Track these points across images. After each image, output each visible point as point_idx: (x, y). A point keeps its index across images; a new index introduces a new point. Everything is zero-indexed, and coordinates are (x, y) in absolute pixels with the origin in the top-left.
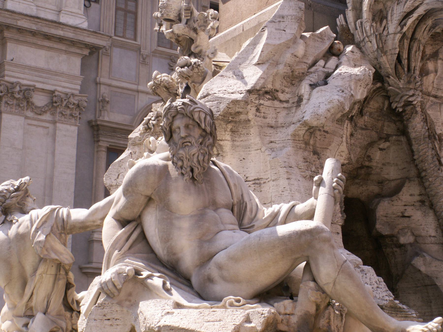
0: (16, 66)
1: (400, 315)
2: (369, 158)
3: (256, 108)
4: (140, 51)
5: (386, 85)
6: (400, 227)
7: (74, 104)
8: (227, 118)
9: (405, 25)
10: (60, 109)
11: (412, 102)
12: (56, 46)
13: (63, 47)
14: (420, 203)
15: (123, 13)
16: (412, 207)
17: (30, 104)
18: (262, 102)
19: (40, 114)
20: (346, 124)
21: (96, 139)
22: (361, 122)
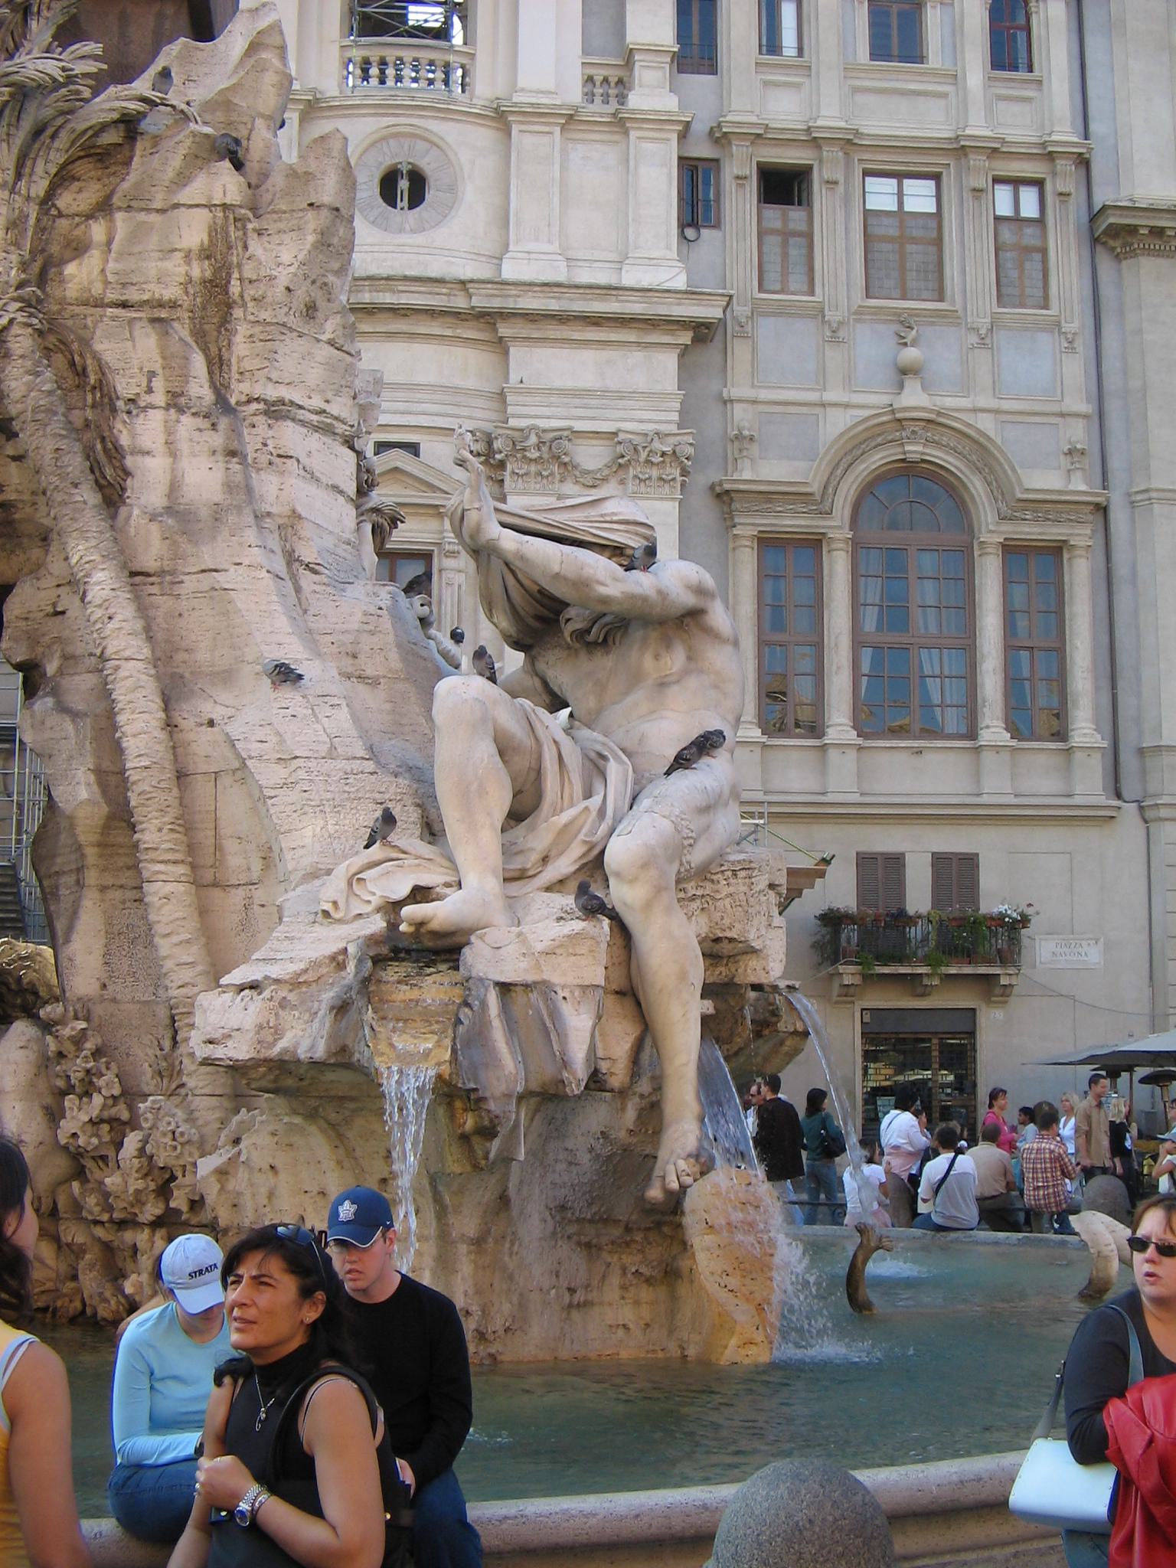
0: (530, 392)
4: (824, 316)
7: (663, 454)
10: (635, 468)
12: (613, 336)
13: (631, 336)
15: (779, 239)
17: (567, 467)
19: (594, 487)
21: (729, 523)
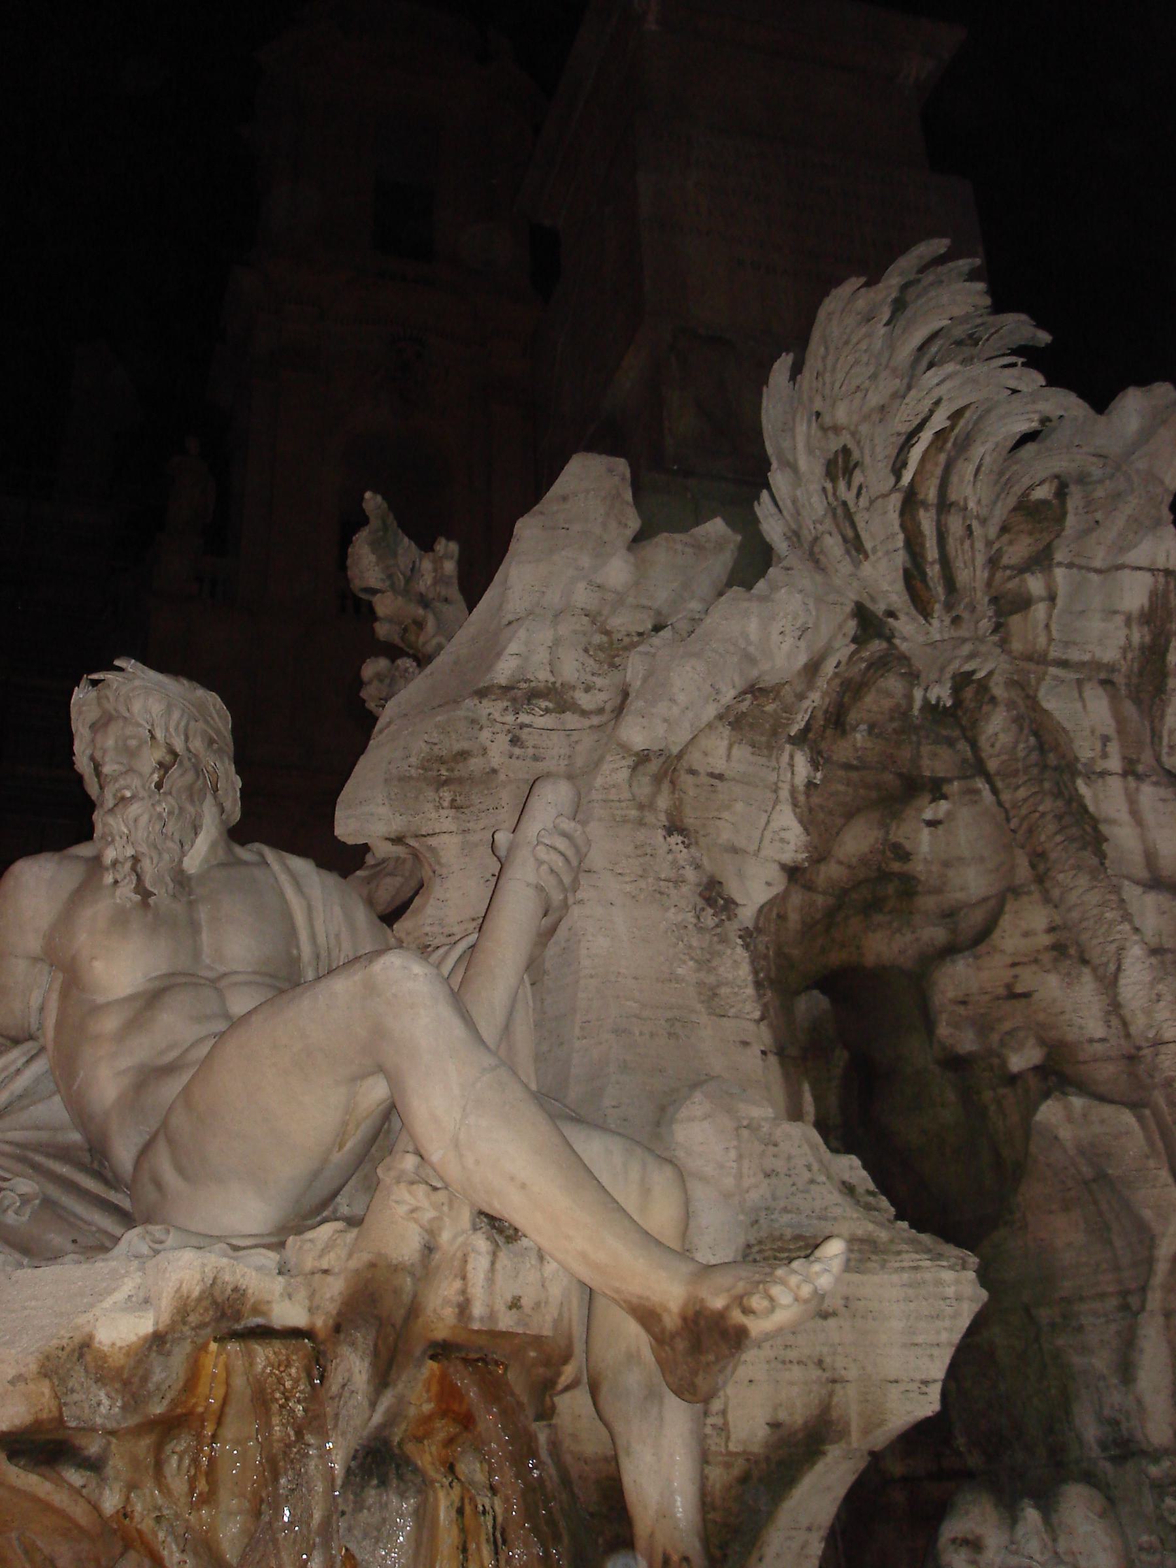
1: (897, 1265)
2: (903, 855)
3: (510, 735)
5: (897, 641)
6: (1007, 1026)
8: (435, 773)
9: (905, 464)
11: (973, 672)
14: (1055, 953)
16: (1034, 968)
18: (524, 718)
20: (785, 758)
22: (843, 750)
